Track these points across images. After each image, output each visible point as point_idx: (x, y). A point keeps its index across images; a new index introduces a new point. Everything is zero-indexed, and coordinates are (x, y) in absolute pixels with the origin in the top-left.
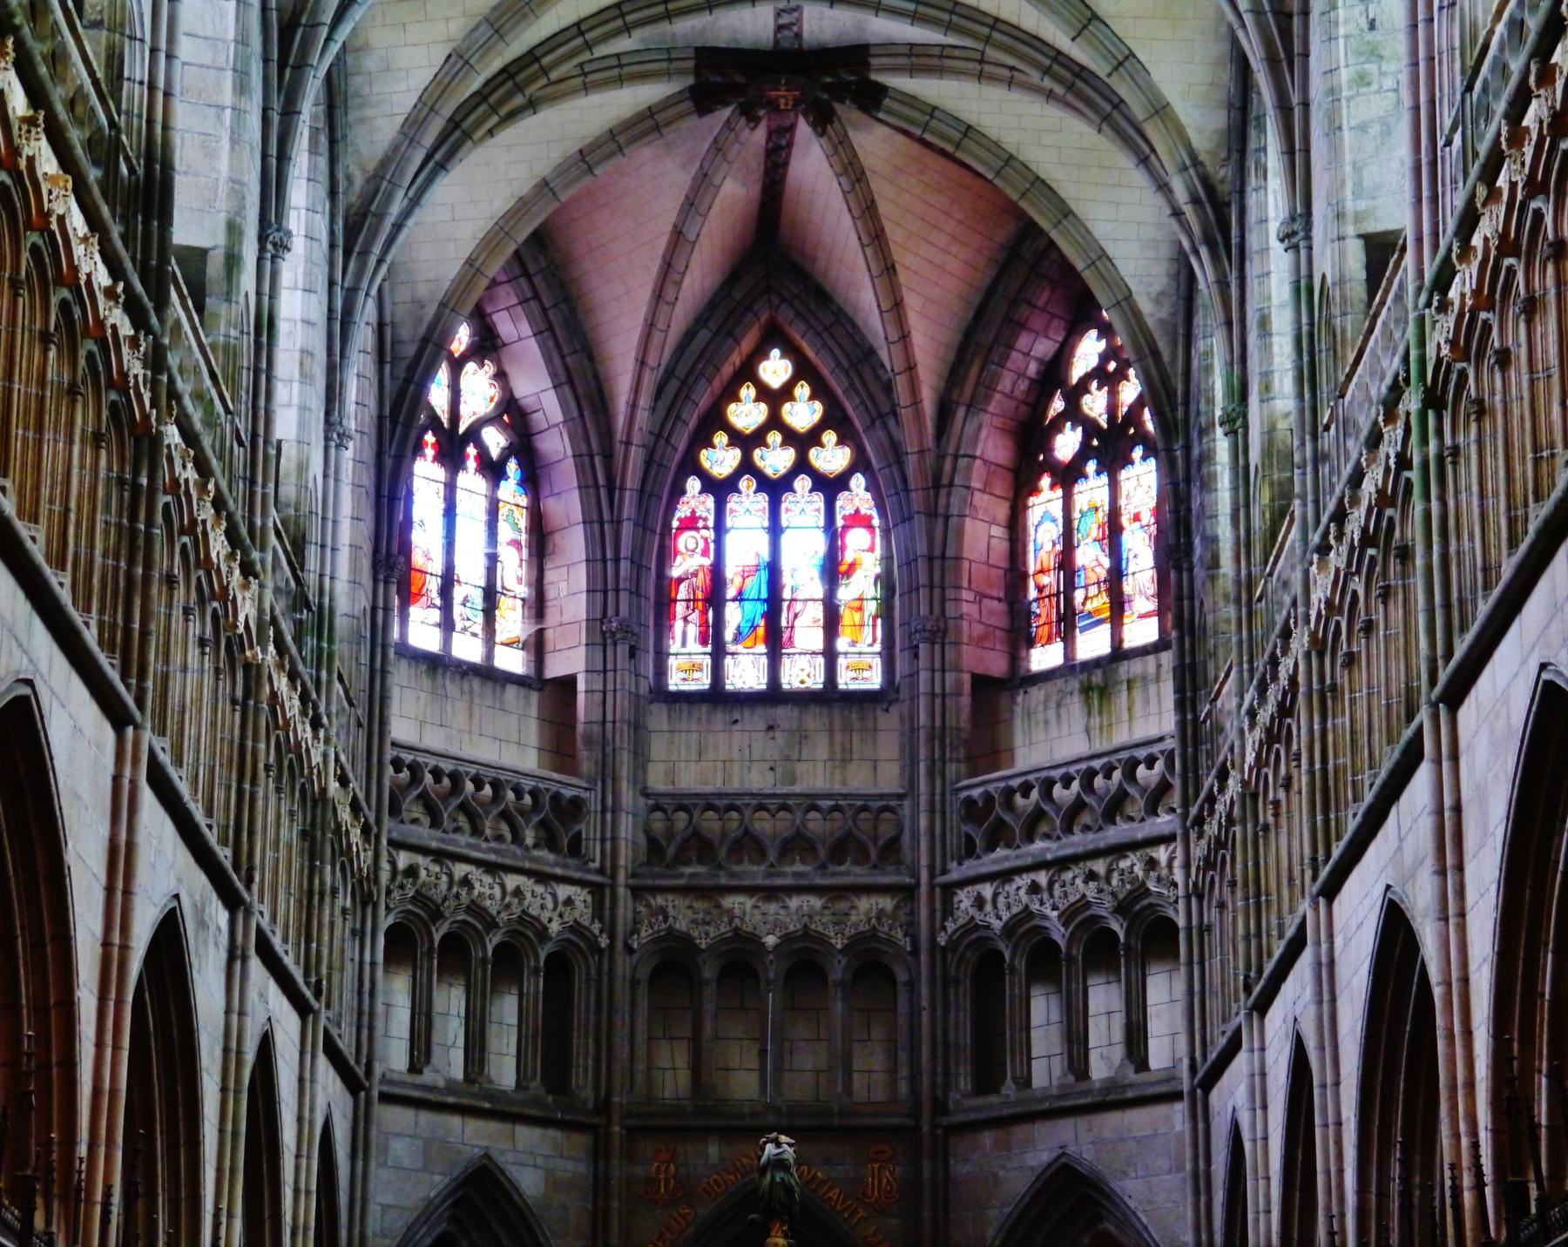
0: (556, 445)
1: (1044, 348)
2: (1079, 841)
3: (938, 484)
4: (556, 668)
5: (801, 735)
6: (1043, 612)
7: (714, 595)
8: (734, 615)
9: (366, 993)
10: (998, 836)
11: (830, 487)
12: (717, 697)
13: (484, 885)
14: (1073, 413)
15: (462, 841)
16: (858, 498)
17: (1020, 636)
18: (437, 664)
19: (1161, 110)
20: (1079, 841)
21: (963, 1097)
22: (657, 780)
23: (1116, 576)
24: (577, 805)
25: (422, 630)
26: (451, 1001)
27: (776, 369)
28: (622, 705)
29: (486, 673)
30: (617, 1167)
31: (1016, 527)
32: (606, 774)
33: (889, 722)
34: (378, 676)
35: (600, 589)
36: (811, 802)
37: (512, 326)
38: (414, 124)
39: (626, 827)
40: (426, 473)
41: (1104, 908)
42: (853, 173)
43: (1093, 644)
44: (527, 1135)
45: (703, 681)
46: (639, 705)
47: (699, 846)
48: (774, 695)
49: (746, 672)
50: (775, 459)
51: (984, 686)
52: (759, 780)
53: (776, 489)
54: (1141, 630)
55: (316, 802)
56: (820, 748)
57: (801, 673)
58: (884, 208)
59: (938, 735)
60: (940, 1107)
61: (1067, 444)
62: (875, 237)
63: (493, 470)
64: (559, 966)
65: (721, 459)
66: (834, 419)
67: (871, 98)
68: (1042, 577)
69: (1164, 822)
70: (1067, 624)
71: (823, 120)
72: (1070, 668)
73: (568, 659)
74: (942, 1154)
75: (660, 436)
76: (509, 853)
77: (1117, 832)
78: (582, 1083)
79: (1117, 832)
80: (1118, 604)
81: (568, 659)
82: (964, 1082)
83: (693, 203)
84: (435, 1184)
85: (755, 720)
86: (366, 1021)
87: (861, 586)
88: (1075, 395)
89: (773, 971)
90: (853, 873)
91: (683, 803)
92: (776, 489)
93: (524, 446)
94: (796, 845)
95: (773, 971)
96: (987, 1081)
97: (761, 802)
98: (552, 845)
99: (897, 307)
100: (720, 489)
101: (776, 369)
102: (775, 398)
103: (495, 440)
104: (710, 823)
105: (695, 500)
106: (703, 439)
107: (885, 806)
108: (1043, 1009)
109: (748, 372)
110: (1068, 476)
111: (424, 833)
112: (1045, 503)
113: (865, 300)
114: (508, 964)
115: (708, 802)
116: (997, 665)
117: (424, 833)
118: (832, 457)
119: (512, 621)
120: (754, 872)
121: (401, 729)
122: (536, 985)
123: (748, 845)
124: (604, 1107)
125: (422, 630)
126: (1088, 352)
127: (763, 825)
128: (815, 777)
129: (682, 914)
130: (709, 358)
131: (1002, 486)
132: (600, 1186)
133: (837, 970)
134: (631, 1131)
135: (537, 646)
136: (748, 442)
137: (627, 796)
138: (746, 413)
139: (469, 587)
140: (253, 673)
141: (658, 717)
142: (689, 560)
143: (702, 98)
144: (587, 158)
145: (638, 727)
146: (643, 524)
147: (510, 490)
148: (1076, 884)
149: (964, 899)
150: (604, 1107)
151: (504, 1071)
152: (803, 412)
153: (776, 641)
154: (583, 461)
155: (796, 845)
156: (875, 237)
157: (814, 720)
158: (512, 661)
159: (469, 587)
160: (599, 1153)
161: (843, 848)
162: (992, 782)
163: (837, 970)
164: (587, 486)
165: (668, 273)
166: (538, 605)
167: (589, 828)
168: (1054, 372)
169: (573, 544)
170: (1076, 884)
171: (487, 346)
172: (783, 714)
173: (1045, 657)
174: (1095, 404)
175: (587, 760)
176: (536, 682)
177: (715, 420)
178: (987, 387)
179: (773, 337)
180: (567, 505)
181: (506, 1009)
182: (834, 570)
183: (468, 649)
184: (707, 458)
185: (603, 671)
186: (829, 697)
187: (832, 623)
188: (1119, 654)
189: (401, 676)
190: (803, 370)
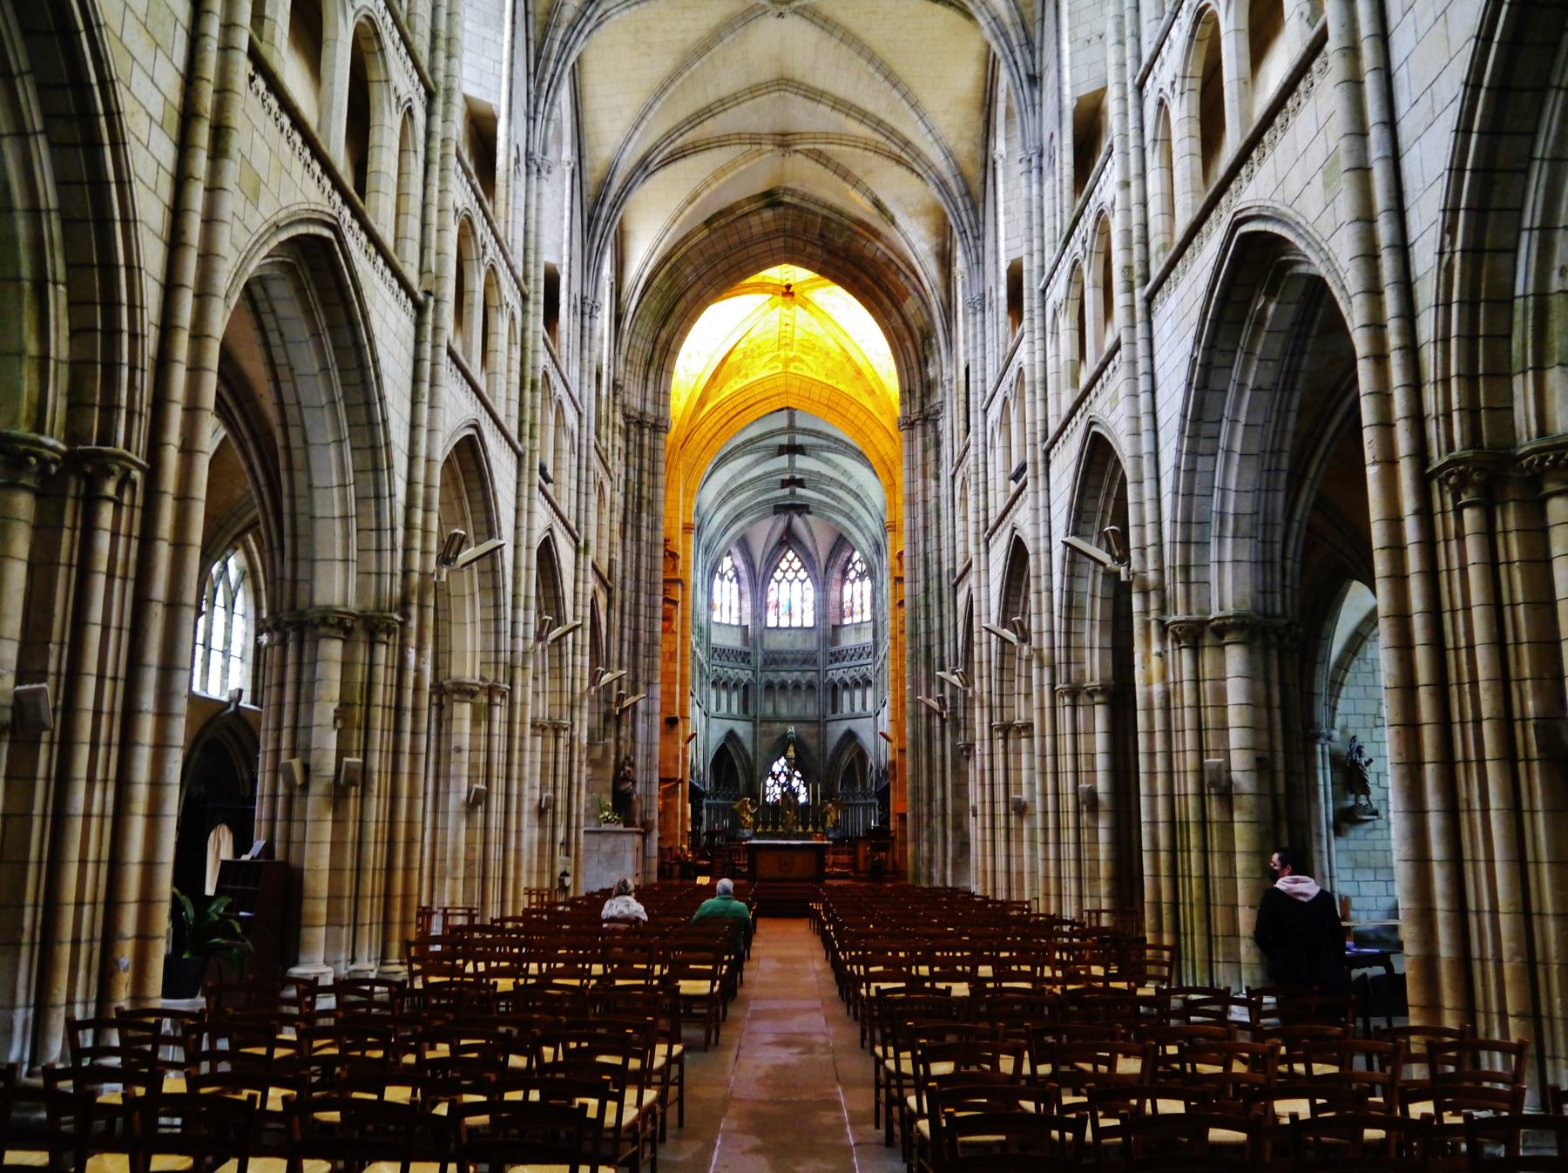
0: (744, 575)
1: (848, 554)
2: (853, 663)
3: (825, 584)
4: (744, 623)
5: (796, 636)
6: (847, 612)
7: (777, 606)
8: (782, 610)
9: (708, 695)
10: (837, 660)
11: (803, 582)
12: (778, 628)
13: (730, 672)
14: (853, 568)
15: (726, 663)
16: (808, 583)
17: (842, 615)
18: (719, 624)
19: (867, 526)
20: (853, 663)
21: (830, 716)
22: (765, 647)
23: (862, 605)
24: (749, 654)
25: (716, 617)
26: (724, 695)
27: (790, 555)
28: (758, 632)
29: (729, 625)
30: (758, 729)
31: (841, 592)
32: (755, 646)
33: (815, 633)
34: (709, 630)
35: (754, 606)
36: (798, 652)
37: (735, 551)
38: (718, 528)
39: (759, 658)
40: (717, 581)
41: (858, 677)
42: (807, 523)
43: (857, 619)
44: (740, 723)
45: (775, 625)
46: (762, 631)
47: (775, 661)
48: (790, 628)
49: (784, 623)
50: (790, 575)
51: (834, 627)
52: (787, 647)
53: (790, 582)
54: (867, 616)
55: (701, 666)
56: (800, 639)
57: (796, 623)
58: (814, 529)
59: (825, 638)
60: (824, 716)
61: (852, 575)
62: (812, 535)
63: (731, 581)
64: (746, 687)
65: (778, 575)
66: (803, 566)
67: (810, 513)
68: (846, 605)
69: (870, 660)
70: (852, 614)
71: (800, 515)
72: (852, 624)
73: (747, 621)
74: (825, 726)
75: (766, 573)
76: (736, 665)
77: (861, 662)
78: (751, 712)
79: (861, 662)
80: (862, 611)
81: (747, 621)
82: (829, 711)
83: (773, 528)
84: (722, 734)
85: (787, 632)
86: (708, 703)
87: (809, 606)
88: (854, 564)
89: (790, 688)
90: (806, 667)
91: (772, 652)
92: (790, 582)
93: (737, 575)
94: (795, 661)
95: (790, 688)
96: (834, 711)
97: (788, 653)
98: (743, 661)
99: (816, 548)
100: (779, 582)
101: (790, 555)
102: (791, 562)
103: (731, 574)
104: (777, 656)
105: (773, 584)
106: (775, 571)
107: (814, 653)
108: (846, 695)
109: (784, 556)
110: (853, 582)
111: (718, 662)
112: (848, 586)
113: (809, 544)
114: (736, 686)
115: (777, 652)
116: (838, 623)
117: (718, 662)
118: (803, 574)
119: (735, 613)
120: (786, 667)
121: (713, 640)
122: (741, 692)
123: (785, 661)
124: (755, 716)
125: (716, 617)
126: (857, 556)
127: (788, 657)
128: (799, 646)
129: (771, 676)
130: (776, 555)
131: (839, 583)
132: (755, 733)
133: (803, 688)
134: (762, 721)
135: (740, 618)
136: (785, 572)
137: (759, 650)
138: (784, 565)
139: (726, 609)
140: (694, 653)
141: (766, 632)
142: (772, 598)
143: (775, 513)
144: (751, 523)
145: (761, 636)
146: (762, 592)
147: (735, 585)
148: (852, 672)
149: (830, 673)
150: (755, 716)
151: (735, 709)
152: (797, 564)
153: (790, 614)
154: (750, 578)
155: (795, 661)
156: (812, 535)
157: (799, 633)
158: (735, 622)
159: (726, 609)
160: (755, 725)
161: (805, 662)
162: (837, 648)
163: (803, 688)
164: (750, 584)
165: (768, 540)
166: (740, 610)
167: (752, 658)
168: (849, 560)
169: (747, 596)
170: (852, 672)
171: (729, 554)
172: (792, 632)
173: (847, 621)
174: (858, 567)
175: (751, 643)
176: (740, 626)
177: (777, 567)
178: (835, 563)
179: (790, 548)
180: (746, 588)
181: (735, 696)
182: (803, 600)
183: (725, 620)
184: (775, 575)
185: (754, 624)
186: (802, 628)
187: (803, 611)
188: (862, 622)
189: (713, 626)
190: (796, 556)
